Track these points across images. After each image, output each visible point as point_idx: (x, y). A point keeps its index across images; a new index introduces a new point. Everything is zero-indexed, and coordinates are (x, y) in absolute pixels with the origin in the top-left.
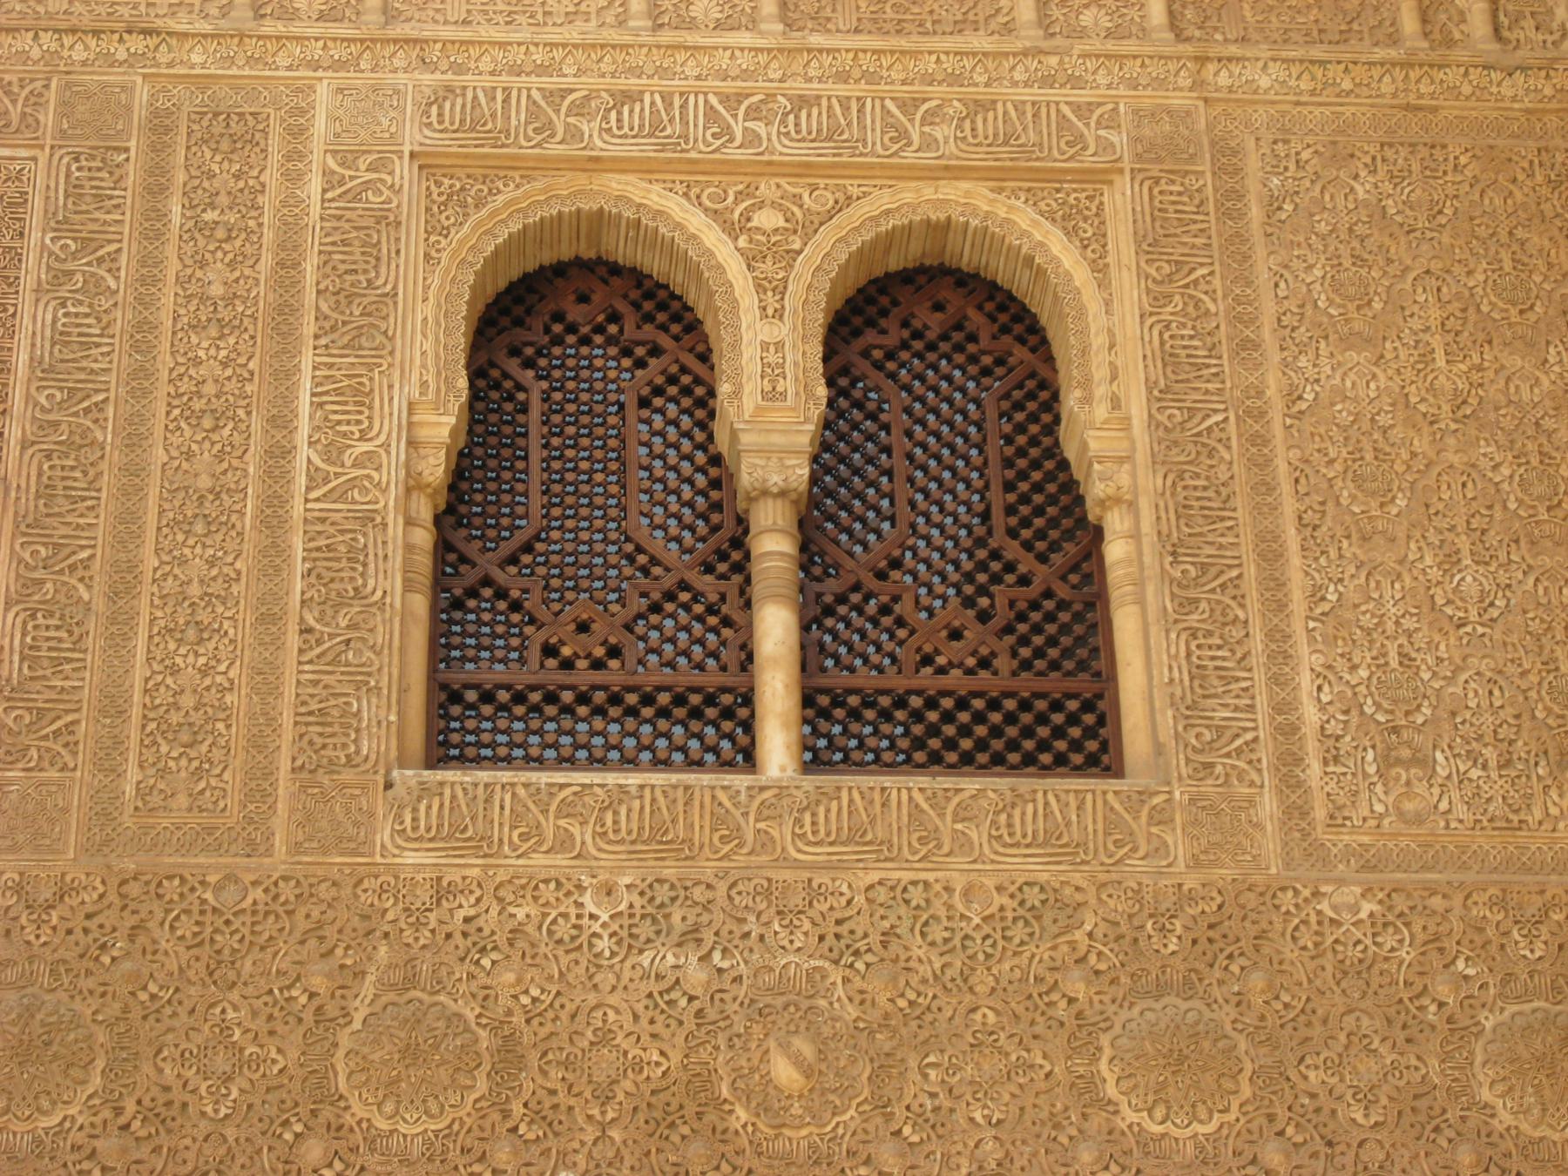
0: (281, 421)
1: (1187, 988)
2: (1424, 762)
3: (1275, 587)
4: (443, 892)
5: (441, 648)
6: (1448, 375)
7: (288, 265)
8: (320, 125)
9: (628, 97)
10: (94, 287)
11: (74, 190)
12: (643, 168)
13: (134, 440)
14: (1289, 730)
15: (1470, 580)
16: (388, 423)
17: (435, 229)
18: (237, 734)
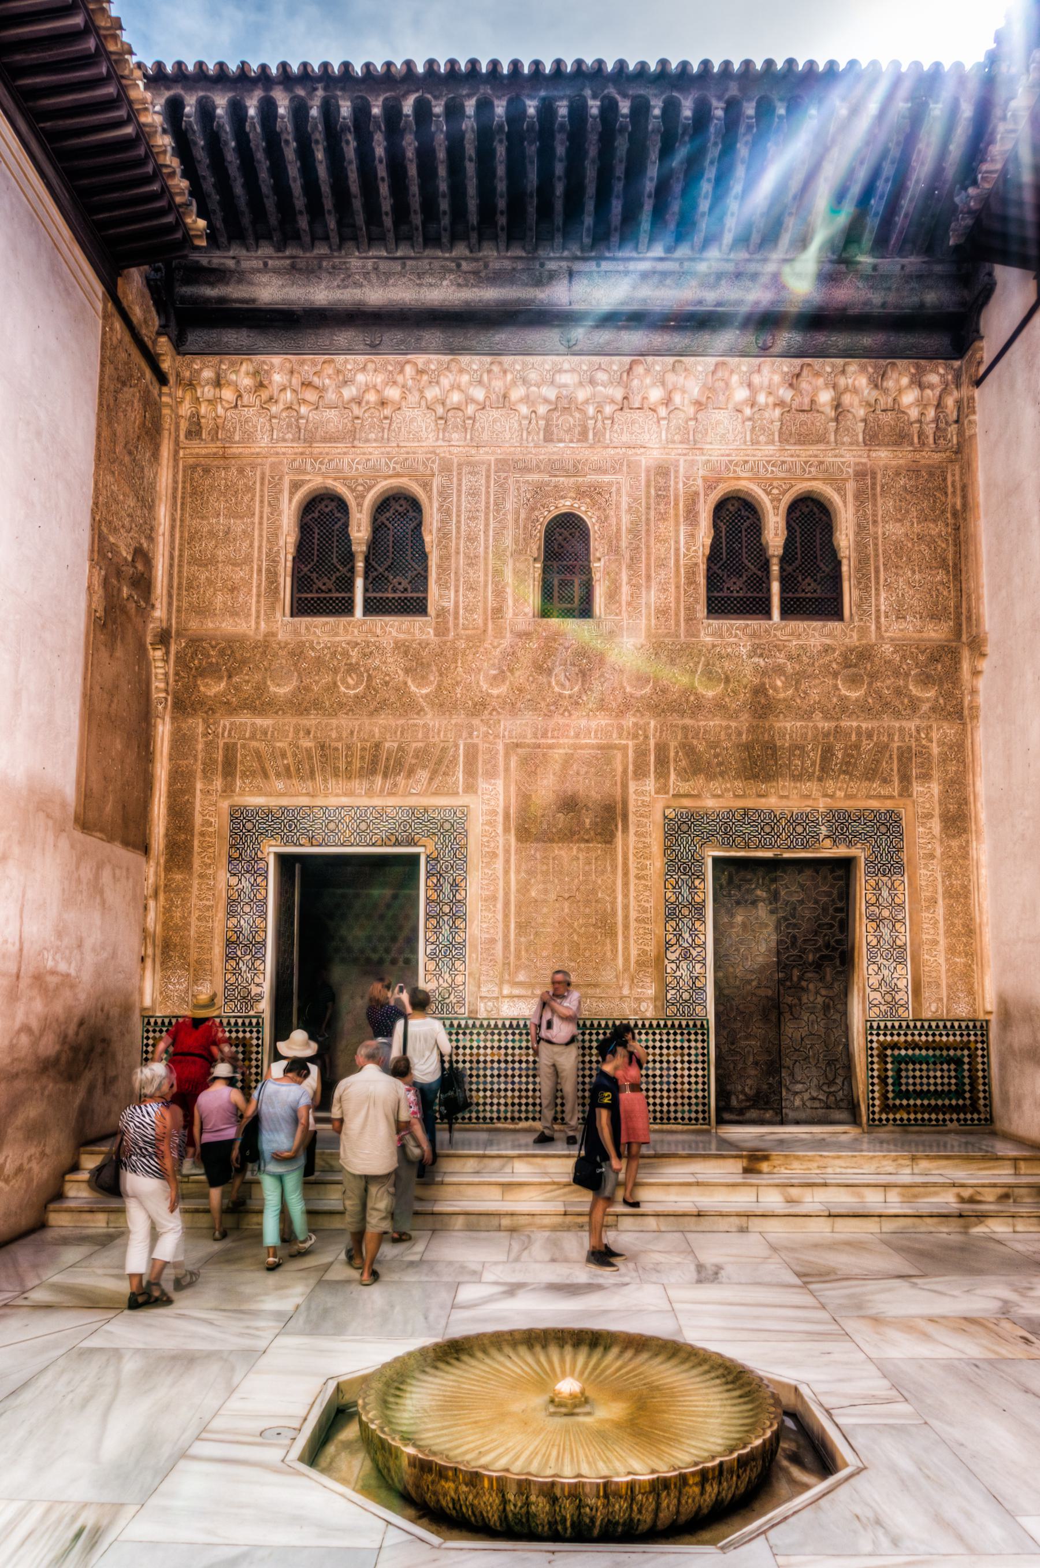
0: (677, 542)
1: (855, 666)
2: (904, 618)
3: (877, 578)
4: (714, 646)
5: (708, 590)
6: (917, 528)
7: (676, 504)
8: (681, 470)
9: (746, 462)
10: (638, 511)
11: (631, 487)
12: (749, 479)
13: (648, 547)
14: (878, 611)
15: (917, 577)
16: (699, 543)
17: (706, 495)
18: (672, 613)
